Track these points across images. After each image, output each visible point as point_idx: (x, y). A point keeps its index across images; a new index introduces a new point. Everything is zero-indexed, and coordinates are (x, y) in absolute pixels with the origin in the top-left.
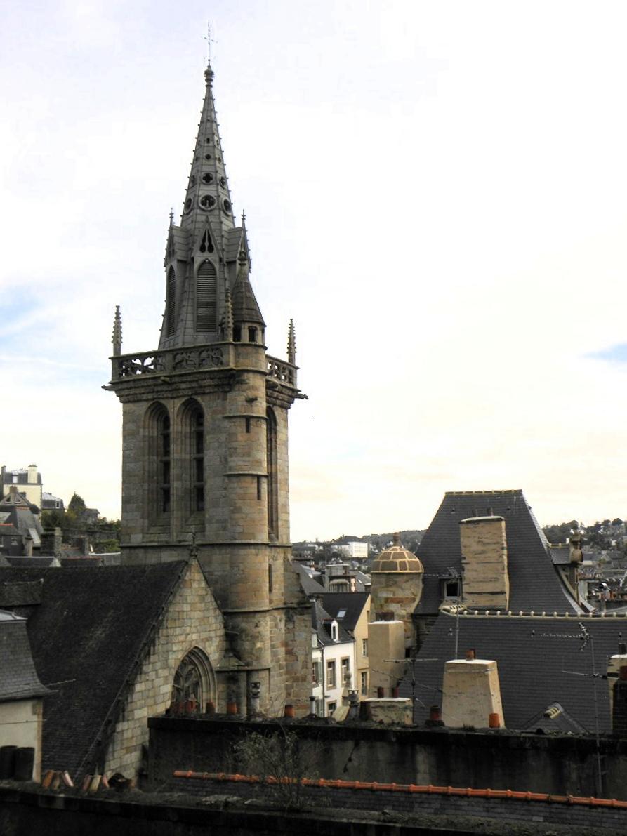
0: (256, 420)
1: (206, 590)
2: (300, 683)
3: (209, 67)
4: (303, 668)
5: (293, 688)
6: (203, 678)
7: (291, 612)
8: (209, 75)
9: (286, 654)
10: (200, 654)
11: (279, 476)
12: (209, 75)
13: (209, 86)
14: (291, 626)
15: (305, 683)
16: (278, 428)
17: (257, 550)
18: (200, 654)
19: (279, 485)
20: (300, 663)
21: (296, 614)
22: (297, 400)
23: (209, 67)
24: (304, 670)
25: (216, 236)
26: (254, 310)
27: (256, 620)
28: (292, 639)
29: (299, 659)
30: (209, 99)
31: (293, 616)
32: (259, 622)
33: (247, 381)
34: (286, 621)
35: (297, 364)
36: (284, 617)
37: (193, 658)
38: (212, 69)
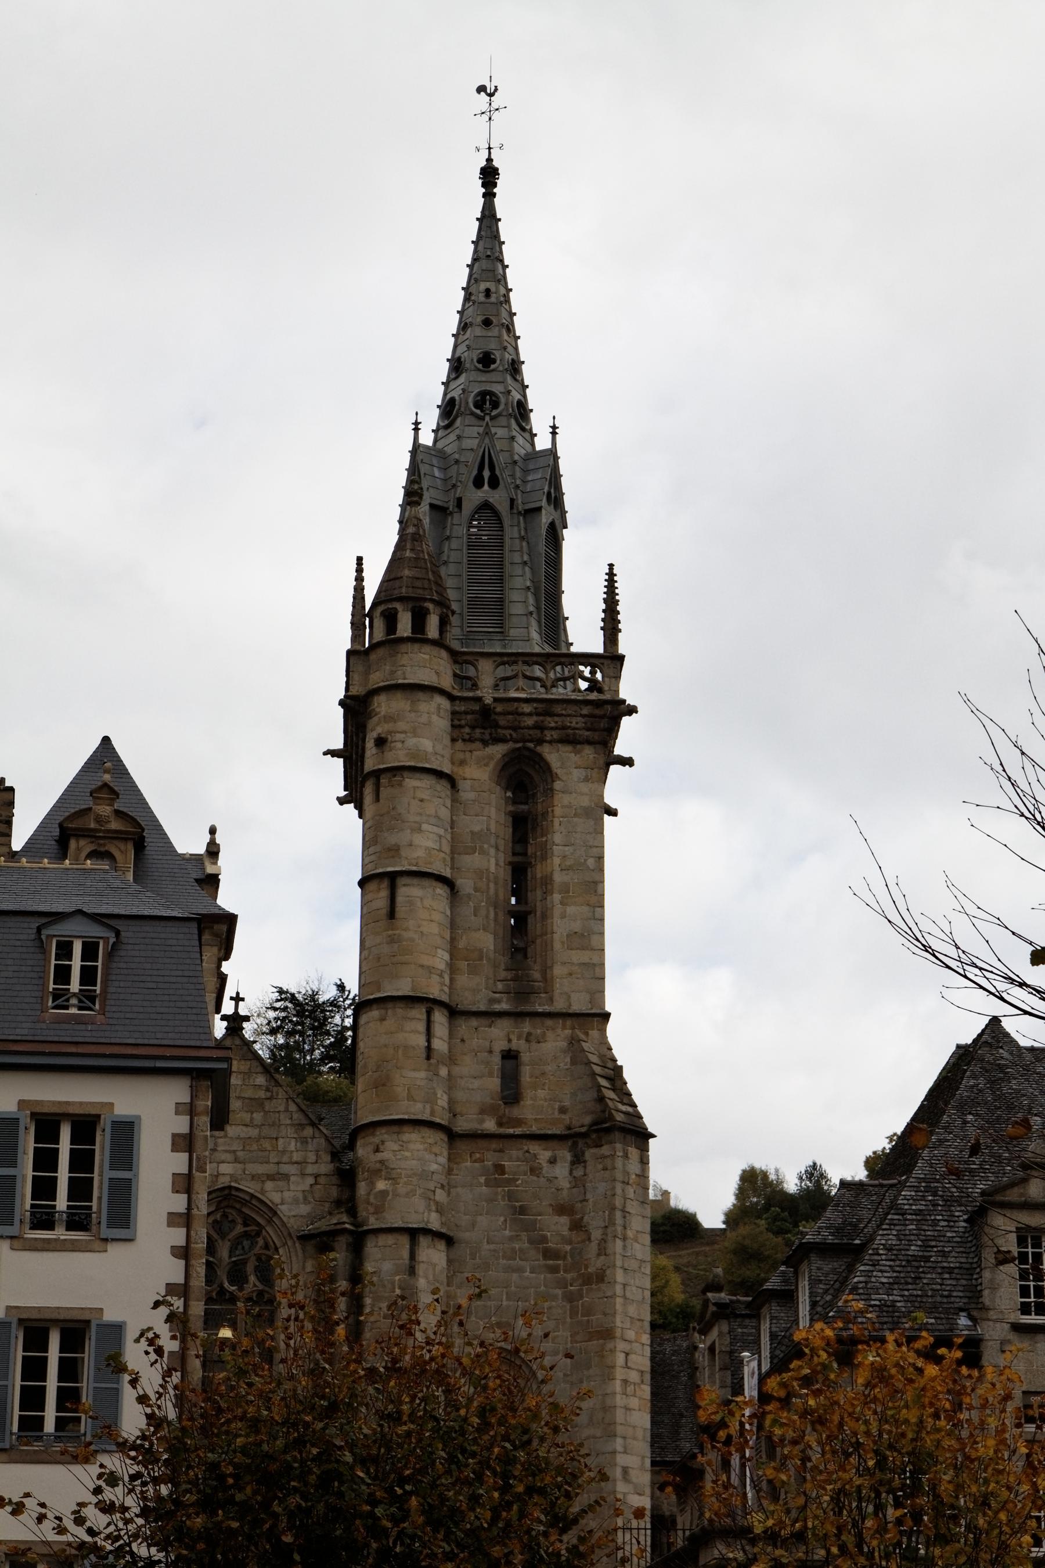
0: (389, 775)
1: (268, 1090)
2: (594, 1286)
3: (489, 160)
4: (599, 1255)
5: (582, 1297)
6: (281, 1251)
7: (581, 1143)
8: (489, 175)
9: (570, 1229)
10: (254, 1202)
11: (559, 878)
12: (489, 175)
13: (489, 196)
14: (579, 1172)
15: (603, 1286)
16: (558, 785)
17: (383, 1011)
18: (254, 1202)
19: (557, 897)
20: (593, 1247)
21: (589, 1147)
22: (625, 721)
23: (489, 160)
24: (602, 1258)
25: (502, 459)
26: (398, 578)
27: (376, 1140)
28: (581, 1198)
29: (592, 1239)
30: (489, 220)
31: (583, 1153)
32: (383, 1142)
33: (378, 710)
34: (573, 1163)
35: (621, 650)
36: (568, 1156)
37: (245, 1210)
38: (495, 163)
